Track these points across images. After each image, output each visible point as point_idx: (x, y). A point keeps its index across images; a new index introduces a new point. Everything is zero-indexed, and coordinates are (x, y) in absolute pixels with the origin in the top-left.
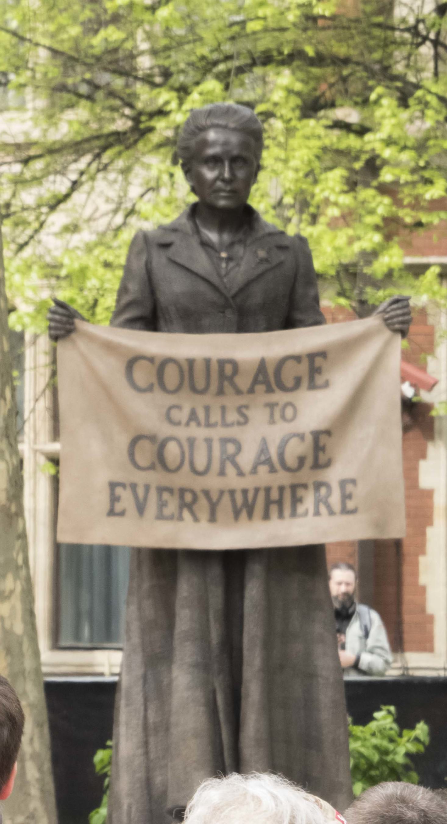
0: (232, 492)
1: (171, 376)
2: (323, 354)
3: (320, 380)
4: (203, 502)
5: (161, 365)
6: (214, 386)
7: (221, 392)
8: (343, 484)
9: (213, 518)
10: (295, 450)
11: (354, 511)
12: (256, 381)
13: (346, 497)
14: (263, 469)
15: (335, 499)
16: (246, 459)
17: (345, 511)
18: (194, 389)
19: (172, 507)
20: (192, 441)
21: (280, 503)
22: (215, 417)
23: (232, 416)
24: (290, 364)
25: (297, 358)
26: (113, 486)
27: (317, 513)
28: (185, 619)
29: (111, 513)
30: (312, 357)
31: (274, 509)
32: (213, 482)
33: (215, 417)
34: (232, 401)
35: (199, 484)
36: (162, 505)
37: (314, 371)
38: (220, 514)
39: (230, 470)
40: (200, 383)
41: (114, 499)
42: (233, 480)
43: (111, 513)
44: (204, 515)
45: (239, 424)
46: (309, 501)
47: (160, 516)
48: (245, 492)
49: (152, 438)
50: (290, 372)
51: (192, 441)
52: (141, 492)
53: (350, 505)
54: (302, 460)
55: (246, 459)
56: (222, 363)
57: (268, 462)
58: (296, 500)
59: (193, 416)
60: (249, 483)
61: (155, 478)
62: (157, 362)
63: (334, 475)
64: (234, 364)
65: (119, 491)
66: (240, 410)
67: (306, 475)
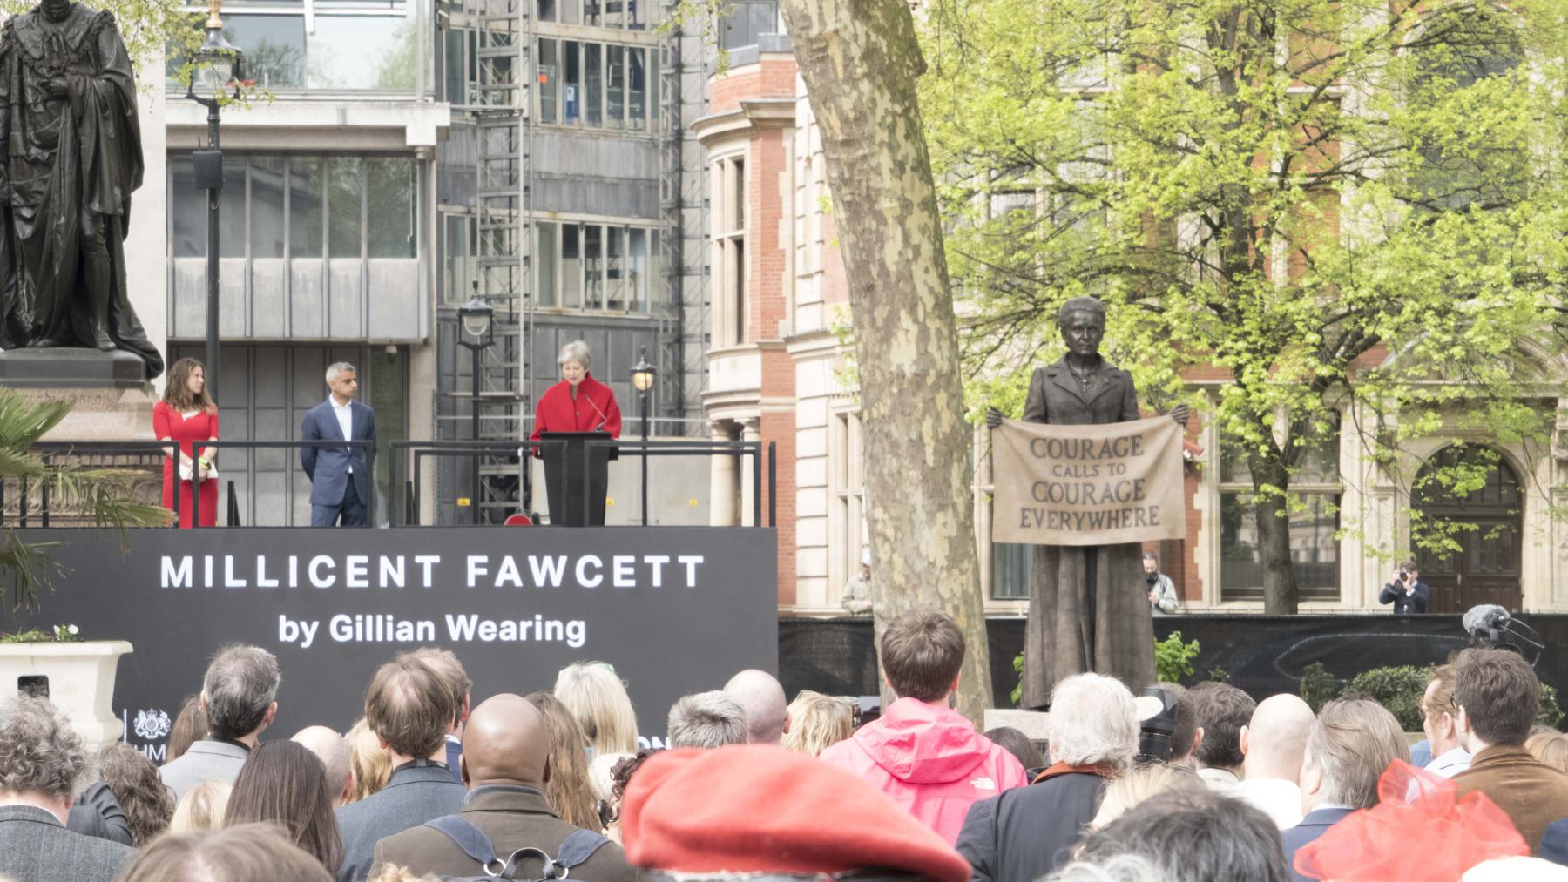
1: (1056, 449)
2: (1140, 436)
3: (1138, 451)
4: (1074, 519)
5: (1050, 443)
6: (1079, 454)
7: (1083, 457)
8: (1151, 508)
9: (1079, 528)
10: (1124, 489)
13: (1153, 516)
14: (1107, 501)
15: (1147, 517)
16: (1098, 495)
17: (1152, 524)
18: (1068, 456)
19: (1057, 521)
20: (1067, 486)
21: (1116, 519)
22: (1080, 471)
23: (1090, 471)
25: (1126, 439)
26: (1024, 510)
28: (1064, 584)
29: (1023, 525)
30: (1134, 438)
32: (1079, 508)
33: (1080, 471)
34: (1089, 463)
35: (1071, 509)
36: (1051, 521)
37: (1135, 445)
39: (1089, 501)
40: (1072, 453)
41: (1024, 518)
42: (1090, 507)
43: (1023, 525)
44: (1074, 526)
46: (1132, 518)
47: (1050, 527)
49: (1045, 483)
50: (1121, 447)
51: (1067, 486)
54: (1128, 495)
55: (1098, 495)
56: (1084, 441)
57: (1110, 496)
58: (1125, 518)
59: (1068, 471)
60: (1099, 508)
61: (1047, 506)
63: (1146, 504)
64: (1091, 442)
66: (1094, 468)
67: (1130, 504)
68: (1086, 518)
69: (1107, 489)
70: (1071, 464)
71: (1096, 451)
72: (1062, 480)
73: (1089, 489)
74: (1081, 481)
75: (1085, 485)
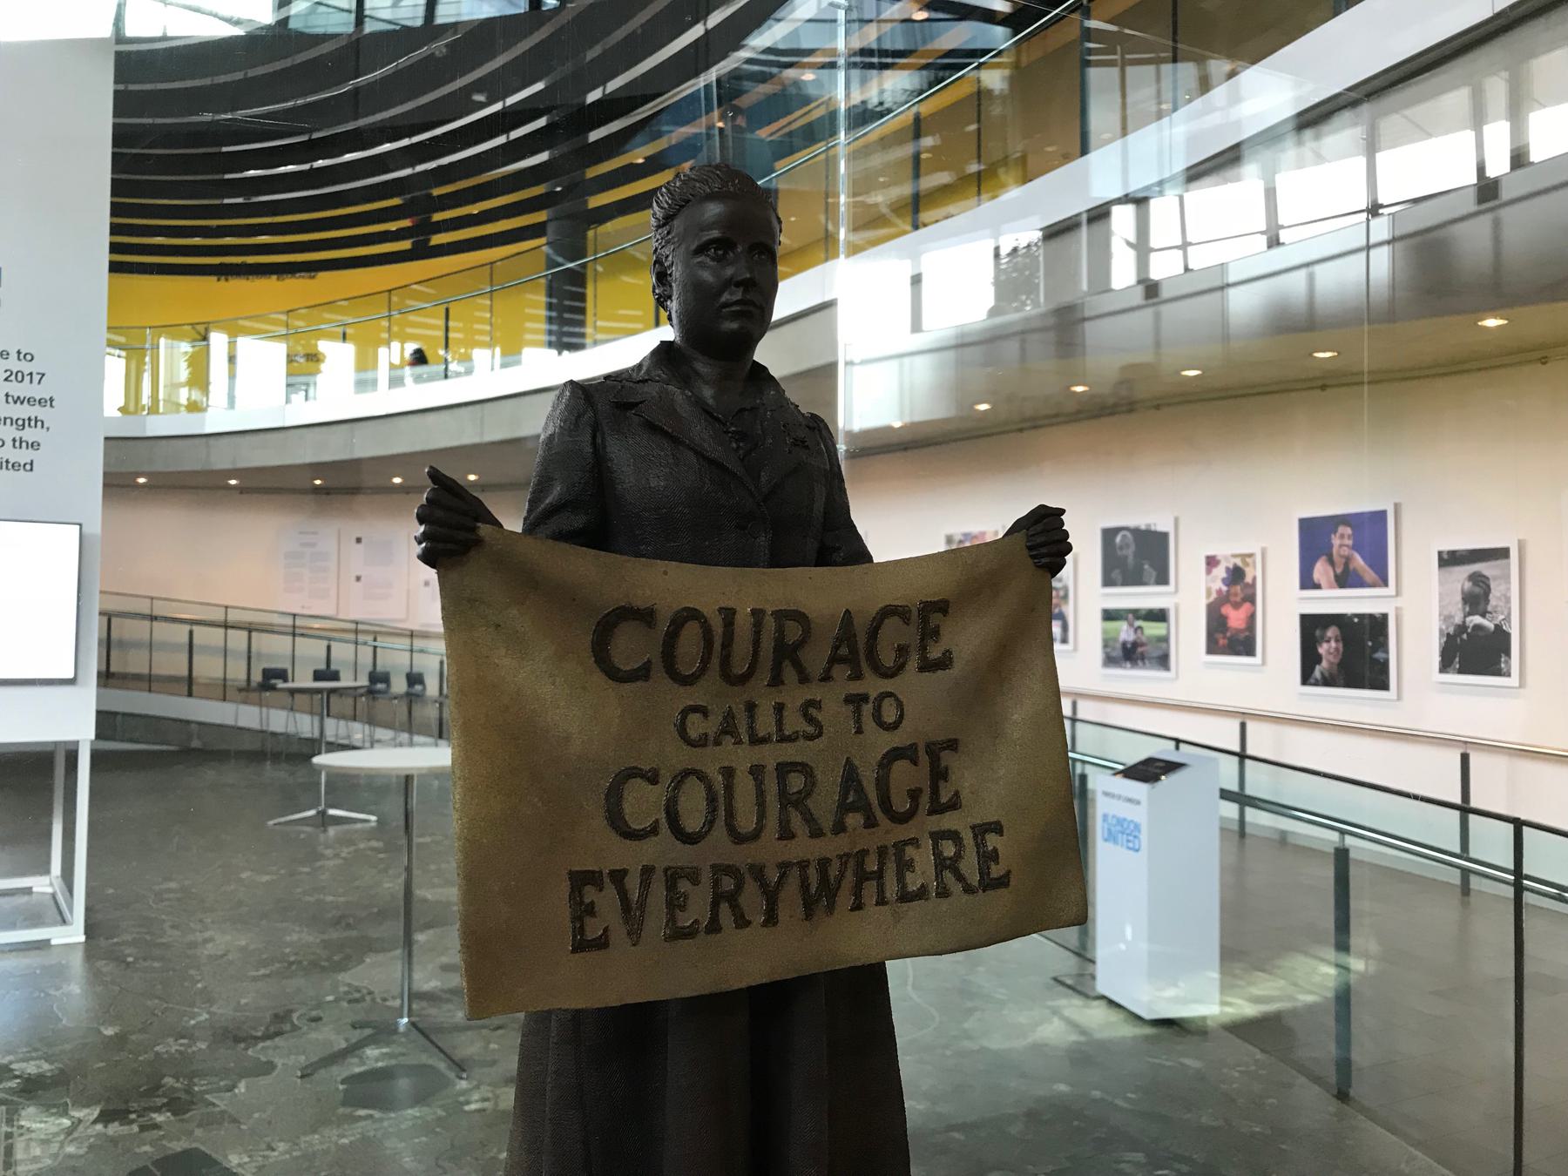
0: (803, 865)
2: (942, 607)
8: (980, 831)
11: (1003, 882)
12: (834, 660)
14: (854, 820)
15: (970, 866)
16: (825, 802)
23: (795, 722)
24: (892, 623)
27: (943, 893)
31: (870, 888)
32: (769, 850)
38: (783, 914)
40: (739, 667)
41: (583, 912)
42: (803, 847)
45: (810, 738)
48: (824, 863)
52: (633, 884)
53: (996, 871)
55: (825, 802)
59: (728, 728)
60: (831, 847)
62: (663, 626)
65: (590, 894)
68: (791, 890)
69: (851, 777)
70: (736, 700)
71: (816, 657)
72: (710, 761)
73: (796, 782)
74: (771, 755)
75: (784, 769)
